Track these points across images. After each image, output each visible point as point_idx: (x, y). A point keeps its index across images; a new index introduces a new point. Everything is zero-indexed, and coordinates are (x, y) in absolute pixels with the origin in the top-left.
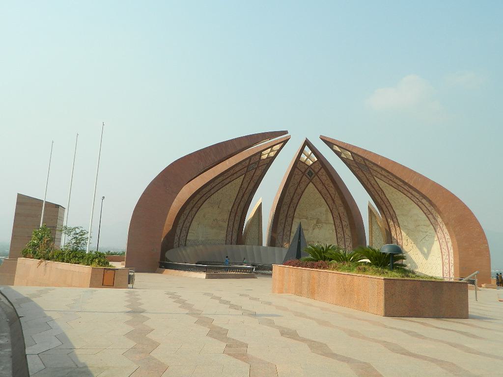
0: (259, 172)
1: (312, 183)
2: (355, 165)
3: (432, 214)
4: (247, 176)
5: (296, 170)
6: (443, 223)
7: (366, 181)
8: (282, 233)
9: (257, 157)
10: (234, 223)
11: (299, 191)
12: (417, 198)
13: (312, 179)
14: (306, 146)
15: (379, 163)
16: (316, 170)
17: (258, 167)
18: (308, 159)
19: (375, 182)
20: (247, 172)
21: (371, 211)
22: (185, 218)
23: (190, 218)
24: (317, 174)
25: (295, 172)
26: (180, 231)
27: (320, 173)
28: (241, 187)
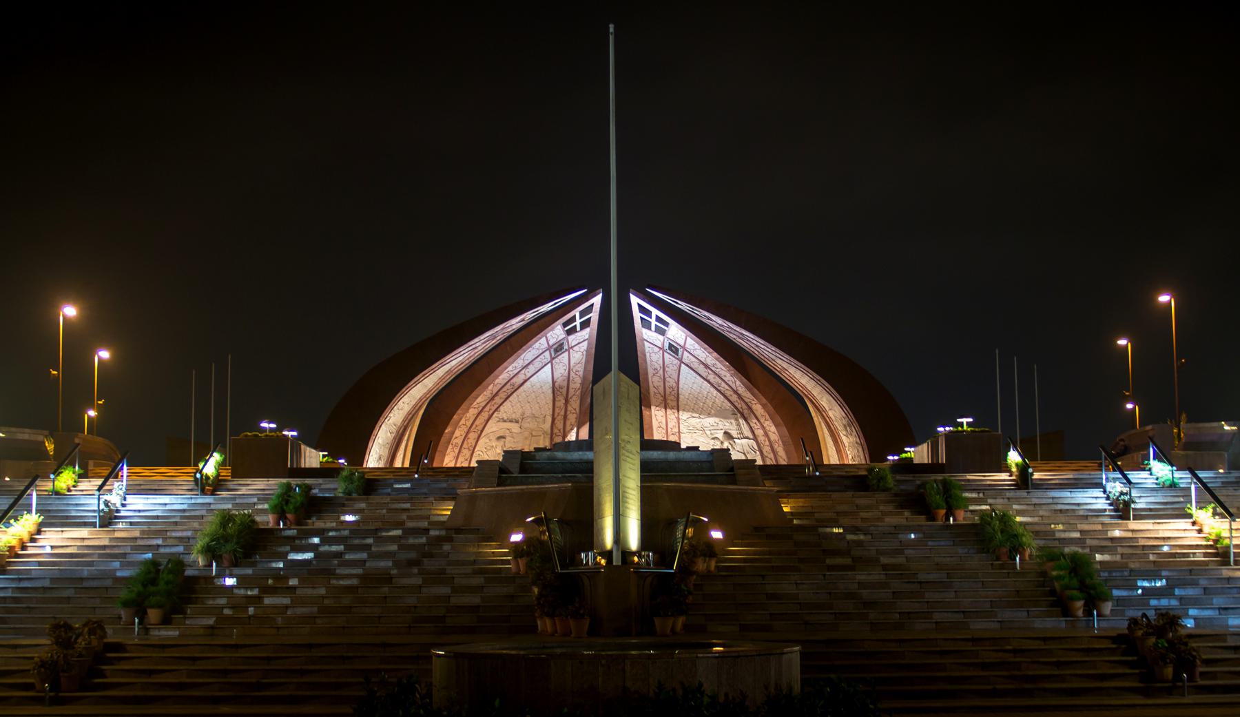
20: (552, 359)
24: (684, 348)
25: (647, 349)
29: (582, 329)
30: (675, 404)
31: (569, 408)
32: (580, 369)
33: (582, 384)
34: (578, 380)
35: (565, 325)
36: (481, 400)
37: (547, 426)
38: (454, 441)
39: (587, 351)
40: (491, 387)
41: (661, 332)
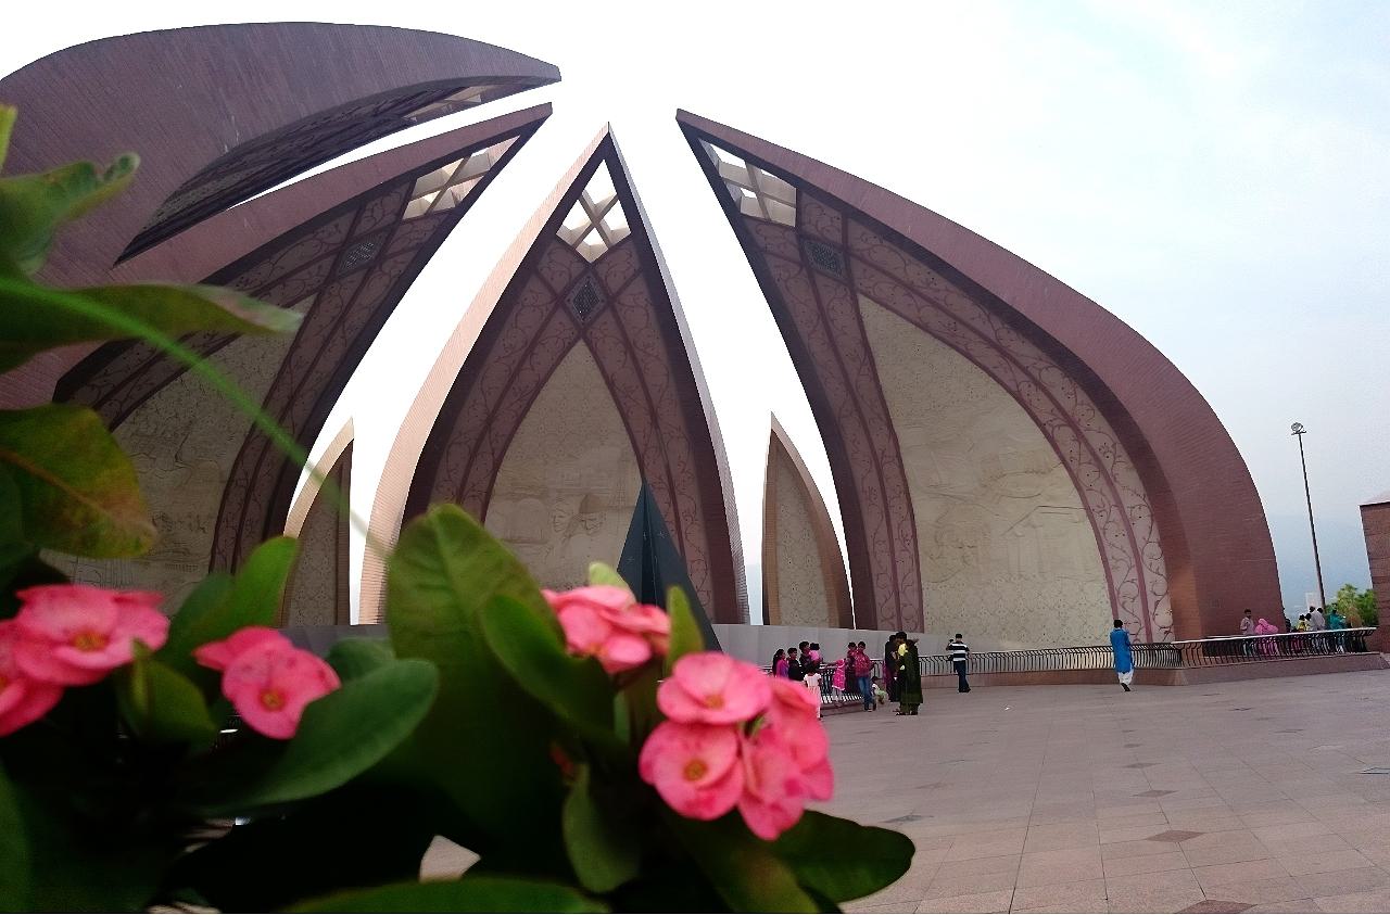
0: (378, 288)
1: (589, 344)
2: (792, 252)
5: (534, 285)
9: (391, 202)
10: (238, 536)
11: (527, 377)
12: (1025, 370)
14: (603, 165)
15: (908, 232)
16: (614, 284)
17: (381, 258)
18: (594, 239)
20: (331, 278)
21: (780, 455)
24: (612, 301)
28: (287, 361)
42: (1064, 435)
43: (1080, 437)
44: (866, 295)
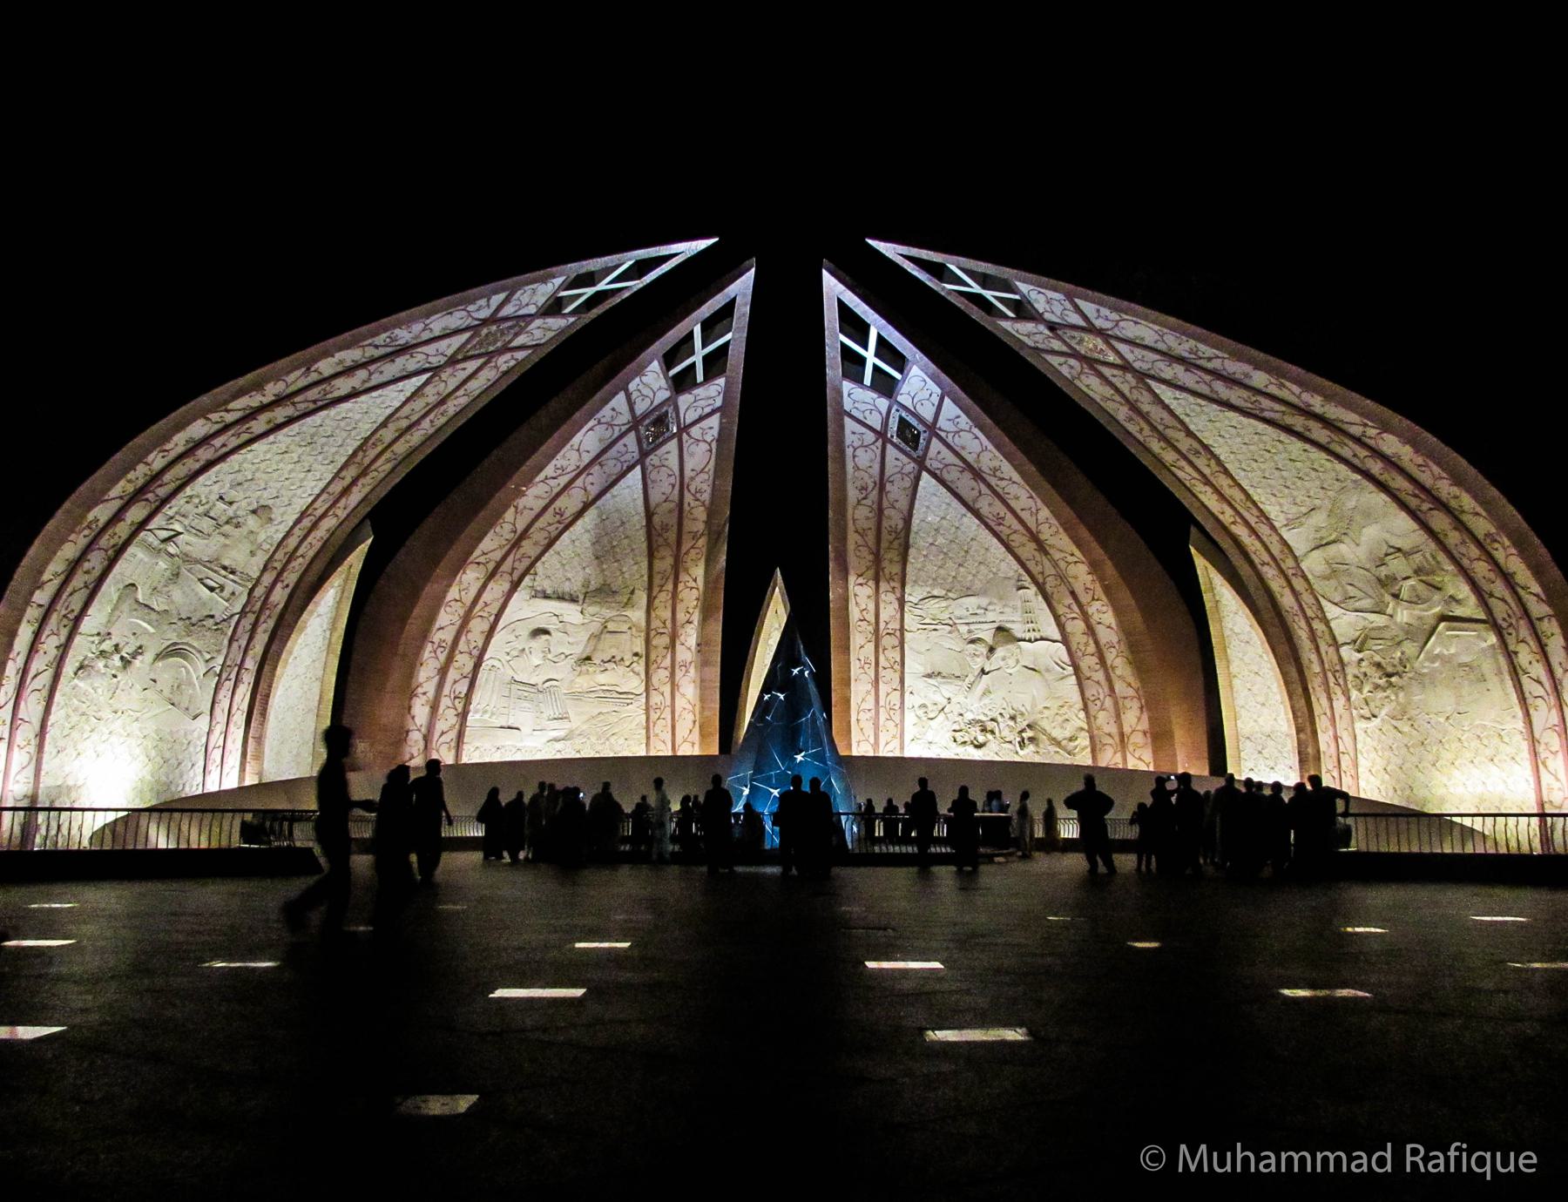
3: (1441, 505)
4: (653, 475)
6: (1507, 543)
7: (1130, 419)
8: (871, 698)
10: (673, 674)
13: (925, 454)
16: (927, 413)
19: (1165, 415)
20: (644, 454)
22: (442, 657)
23: (464, 662)
24: (932, 428)
25: (849, 439)
26: (427, 709)
27: (942, 423)
29: (708, 377)
30: (896, 569)
31: (683, 577)
32: (703, 485)
33: (708, 523)
34: (701, 514)
35: (669, 359)
36: (491, 545)
37: (638, 615)
38: (437, 636)
39: (720, 440)
40: (509, 515)
41: (884, 385)
42: (1440, 521)
43: (1460, 525)
44: (1153, 378)
